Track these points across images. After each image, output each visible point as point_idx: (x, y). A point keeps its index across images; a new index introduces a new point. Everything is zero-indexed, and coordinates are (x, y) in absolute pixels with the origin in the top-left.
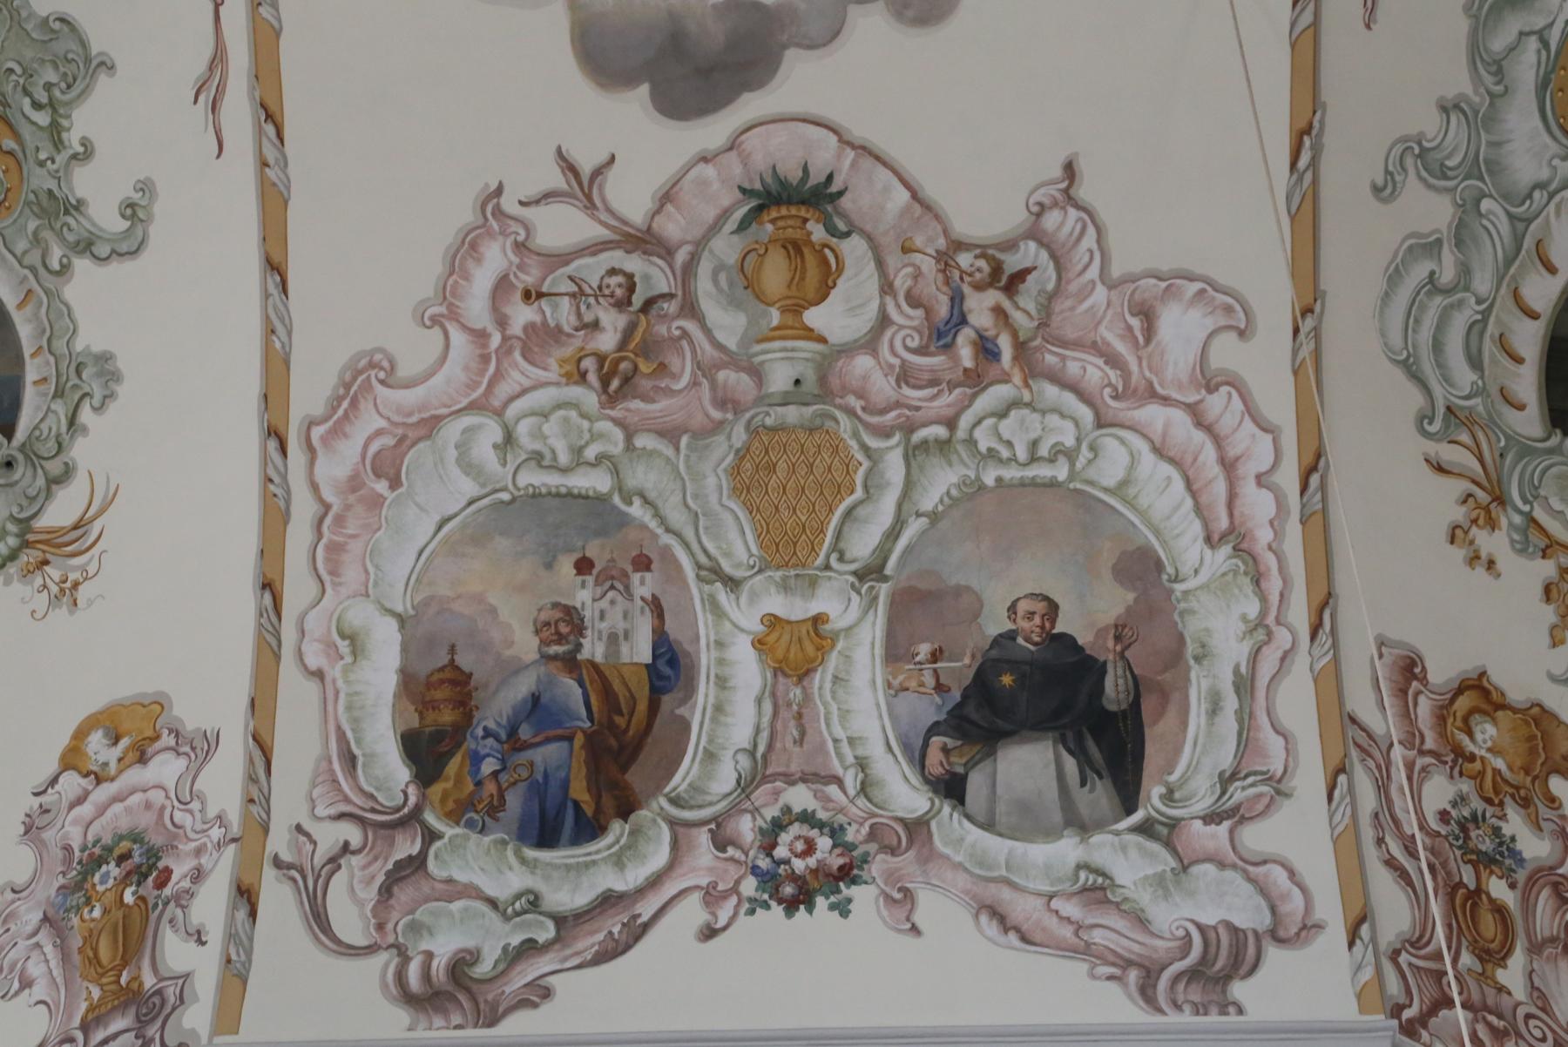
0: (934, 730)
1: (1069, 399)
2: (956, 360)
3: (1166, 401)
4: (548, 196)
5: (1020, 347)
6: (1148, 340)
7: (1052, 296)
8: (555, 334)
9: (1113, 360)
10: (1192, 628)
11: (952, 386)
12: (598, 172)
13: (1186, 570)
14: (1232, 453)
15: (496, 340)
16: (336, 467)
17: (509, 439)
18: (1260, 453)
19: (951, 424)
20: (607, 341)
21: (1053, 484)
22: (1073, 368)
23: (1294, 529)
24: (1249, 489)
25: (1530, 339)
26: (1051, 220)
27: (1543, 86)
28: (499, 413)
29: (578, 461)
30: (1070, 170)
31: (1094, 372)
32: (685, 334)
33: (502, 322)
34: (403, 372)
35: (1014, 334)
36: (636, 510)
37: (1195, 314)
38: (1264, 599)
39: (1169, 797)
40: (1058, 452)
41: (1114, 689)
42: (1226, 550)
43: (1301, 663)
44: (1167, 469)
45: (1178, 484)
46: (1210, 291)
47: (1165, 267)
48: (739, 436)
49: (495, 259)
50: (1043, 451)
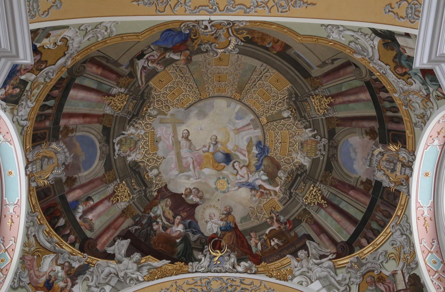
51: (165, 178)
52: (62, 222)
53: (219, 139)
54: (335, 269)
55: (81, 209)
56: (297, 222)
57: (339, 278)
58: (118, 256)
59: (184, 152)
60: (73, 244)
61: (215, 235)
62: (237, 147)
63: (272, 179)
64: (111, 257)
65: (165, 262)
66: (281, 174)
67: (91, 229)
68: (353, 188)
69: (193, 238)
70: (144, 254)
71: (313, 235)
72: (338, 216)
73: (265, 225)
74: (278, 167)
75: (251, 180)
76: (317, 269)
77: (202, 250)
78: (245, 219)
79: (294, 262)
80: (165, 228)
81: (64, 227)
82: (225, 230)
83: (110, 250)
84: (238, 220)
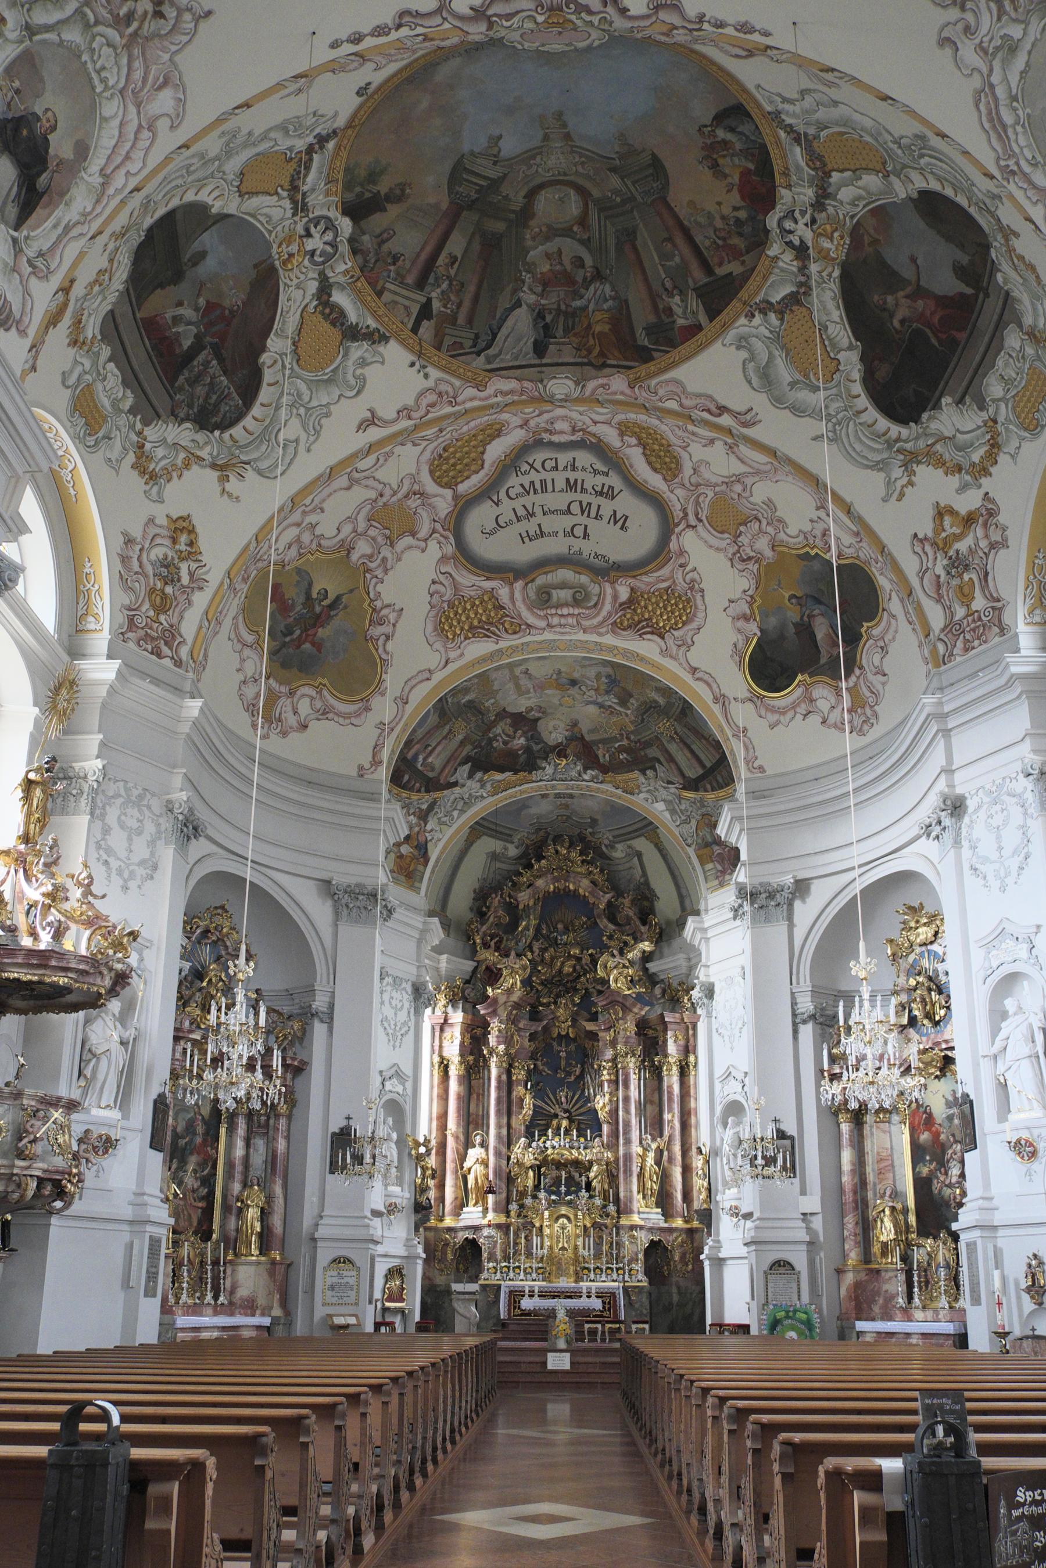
1: (125, 71)
2: (120, 8)
3: (139, 113)
5: (135, 34)
6: (156, 90)
7: (159, 36)
9: (145, 80)
10: (74, 191)
11: (111, 12)
13: (89, 171)
14: (132, 155)
18: (134, 167)
19: (97, 23)
21: (93, 88)
22: (136, 64)
23: (119, 198)
24: (122, 171)
25: (175, 202)
26: (187, 16)
27: (258, 154)
30: (209, 13)
31: (138, 75)
35: (140, 28)
37: (172, 103)
38: (93, 209)
39: (27, 238)
40: (104, 81)
41: (43, 180)
42: (101, 180)
43: (83, 241)
44: (117, 133)
45: (113, 142)
46: (181, 103)
47: (185, 79)
50: (103, 74)
51: (503, 703)
52: (406, 777)
53: (563, 669)
54: (680, 798)
55: (421, 758)
56: (648, 744)
57: (683, 807)
58: (461, 781)
59: (524, 682)
60: (419, 791)
61: (560, 744)
62: (583, 676)
63: (623, 703)
64: (455, 784)
65: (508, 774)
66: (632, 701)
67: (433, 769)
68: (706, 739)
69: (536, 748)
70: (486, 771)
71: (662, 759)
72: (689, 755)
73: (614, 740)
74: (631, 696)
75: (600, 700)
76: (663, 794)
77: (546, 759)
78: (591, 731)
79: (642, 779)
80: (505, 743)
81: (409, 781)
82: (570, 739)
83: (452, 780)
84: (584, 731)
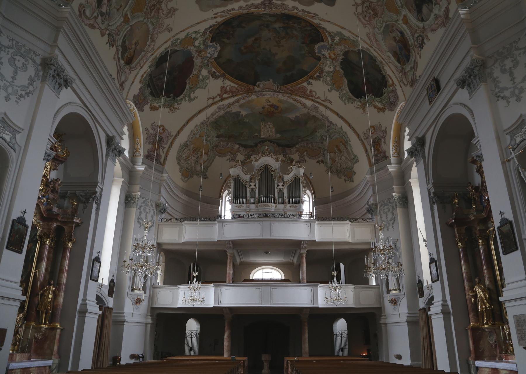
0: (418, 15)
4: (356, 9)
8: (370, 17)
12: (355, 3)
15: (369, 23)
16: (375, 45)
17: (377, 28)
20: (372, 13)
28: (375, 28)
29: (382, 24)
32: (374, 5)
33: (367, 21)
34: (369, 32)
36: (388, 23)
48: (385, 7)
49: (361, 17)
